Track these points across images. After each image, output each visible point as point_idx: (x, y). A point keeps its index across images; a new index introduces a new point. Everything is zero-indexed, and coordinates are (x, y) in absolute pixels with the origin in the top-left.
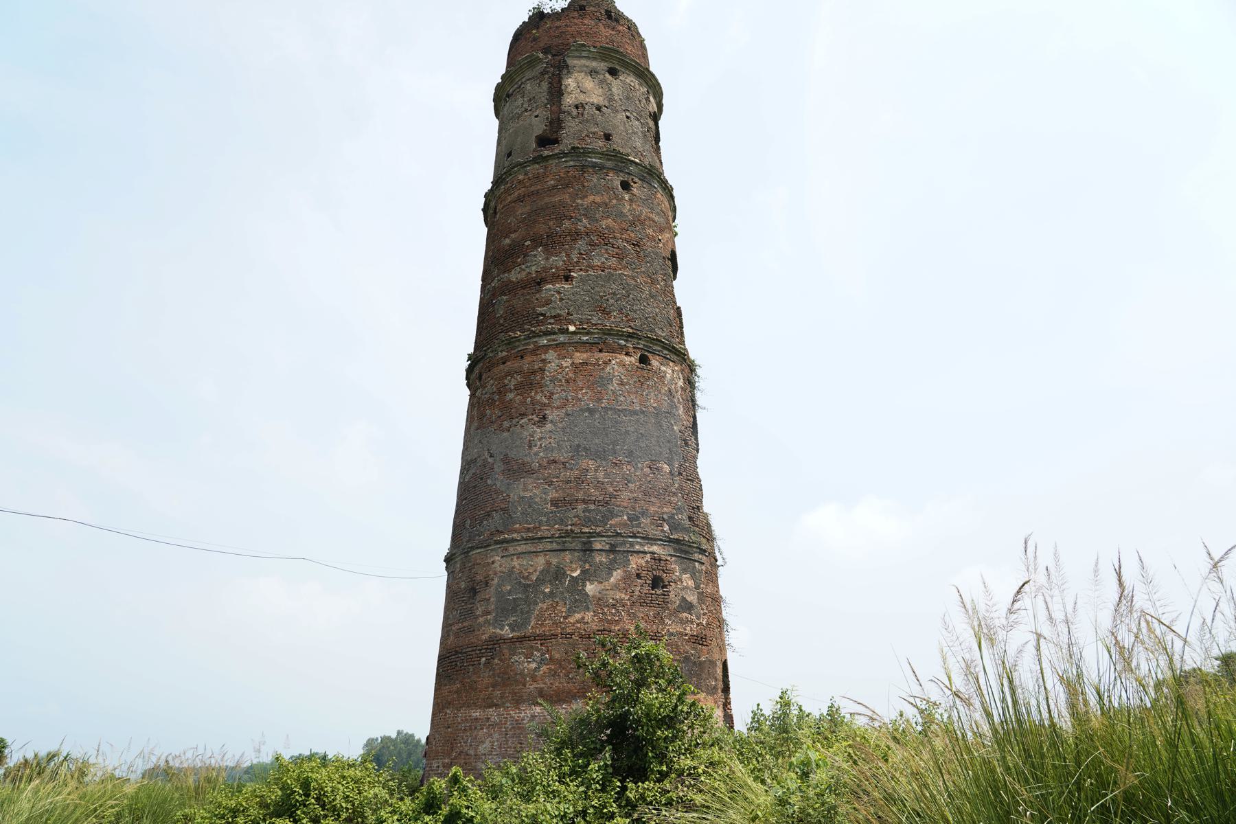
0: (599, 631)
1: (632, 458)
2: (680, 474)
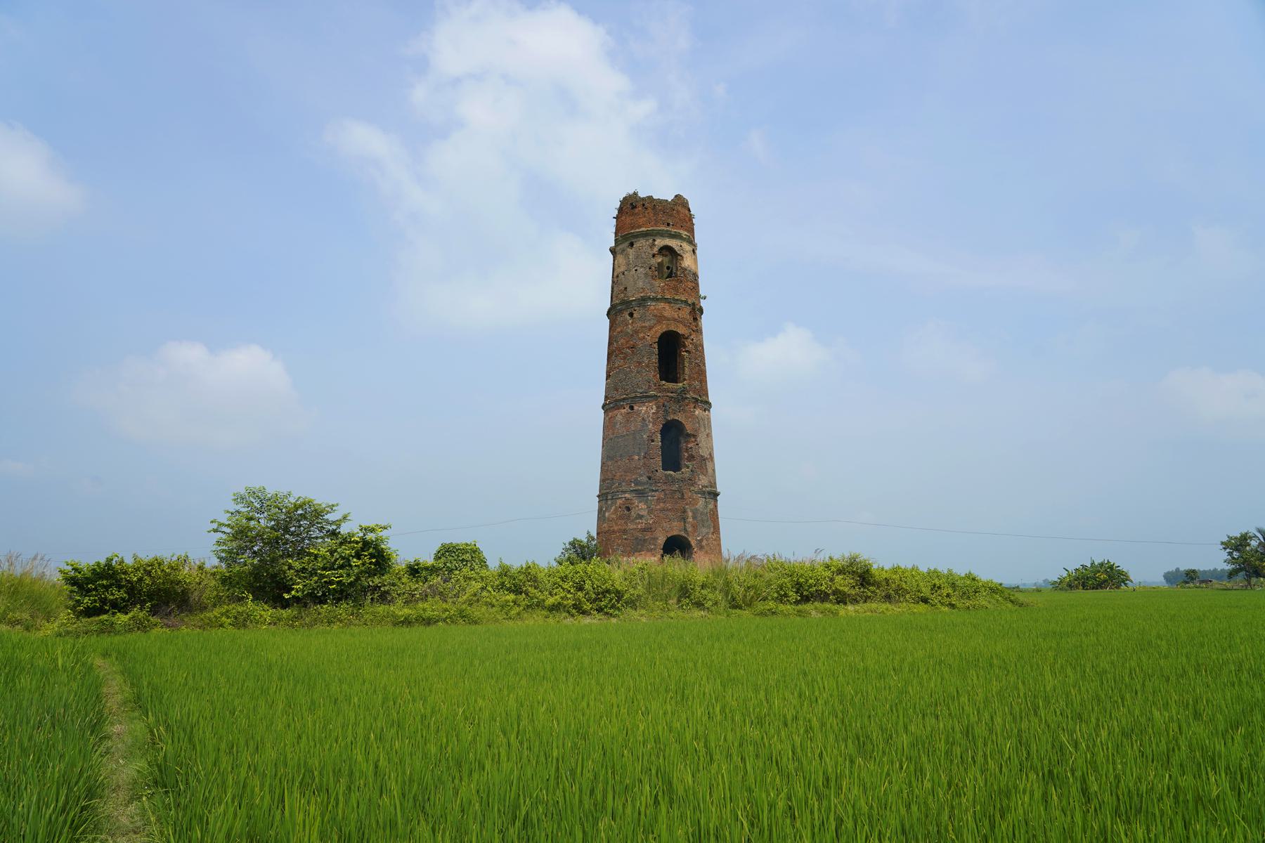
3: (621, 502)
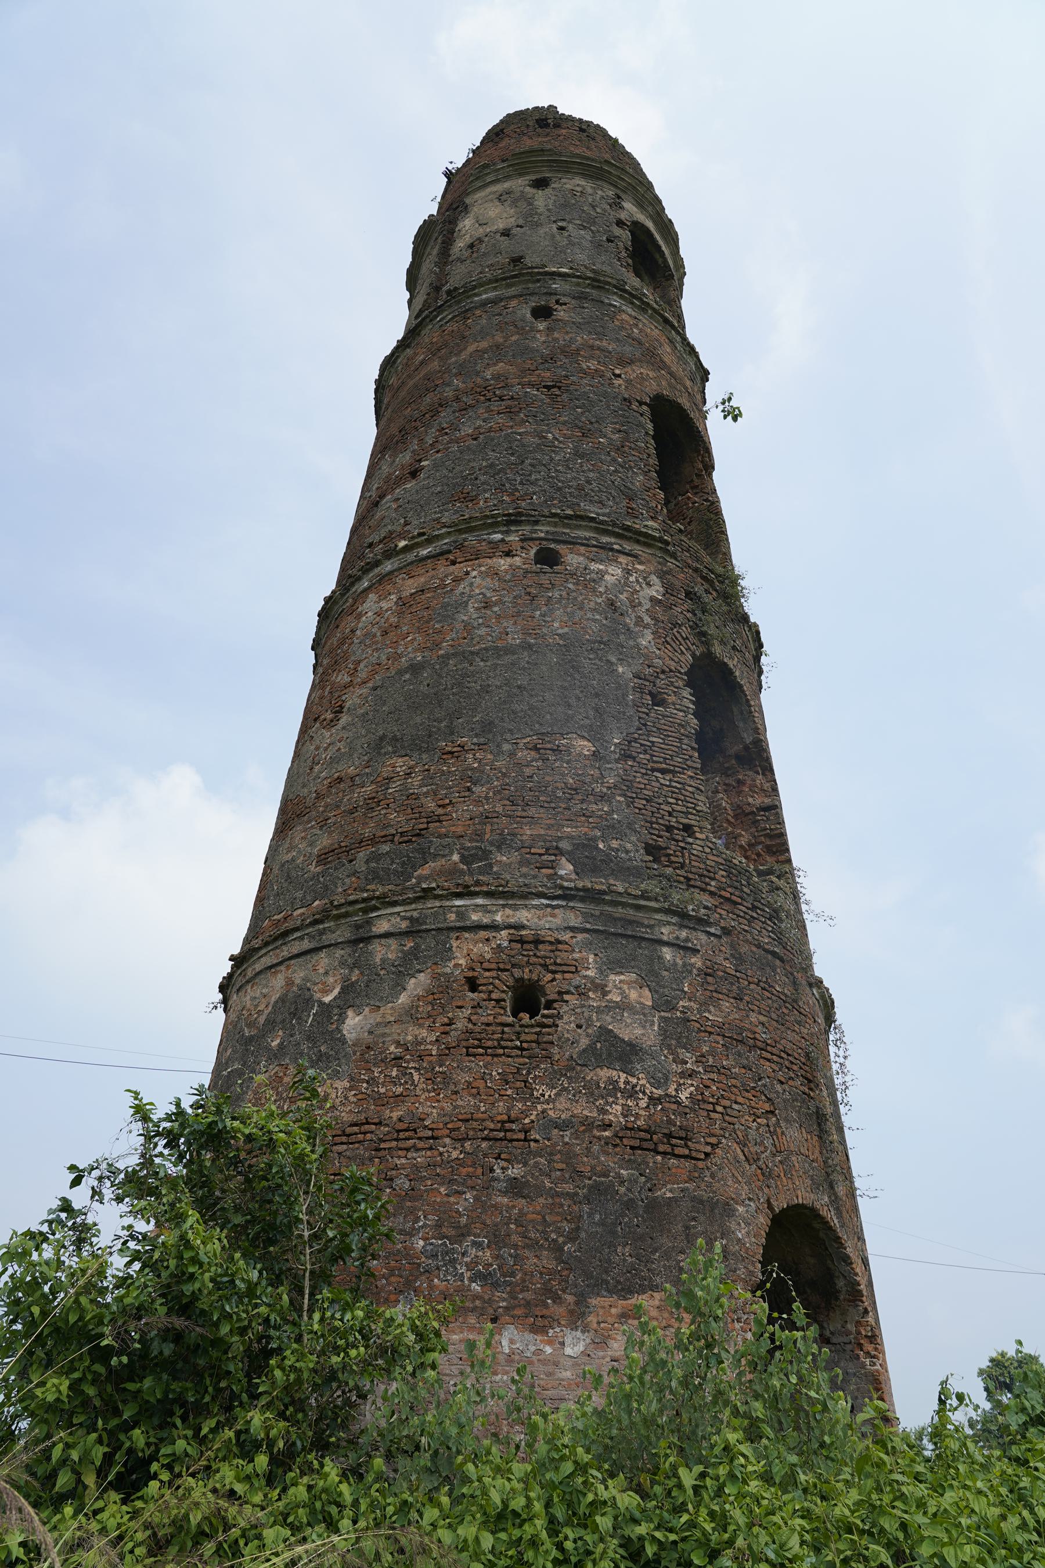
0: (355, 1125)
1: (490, 736)
2: (626, 756)
3: (486, 951)
